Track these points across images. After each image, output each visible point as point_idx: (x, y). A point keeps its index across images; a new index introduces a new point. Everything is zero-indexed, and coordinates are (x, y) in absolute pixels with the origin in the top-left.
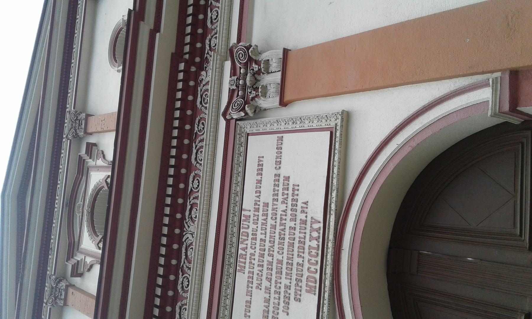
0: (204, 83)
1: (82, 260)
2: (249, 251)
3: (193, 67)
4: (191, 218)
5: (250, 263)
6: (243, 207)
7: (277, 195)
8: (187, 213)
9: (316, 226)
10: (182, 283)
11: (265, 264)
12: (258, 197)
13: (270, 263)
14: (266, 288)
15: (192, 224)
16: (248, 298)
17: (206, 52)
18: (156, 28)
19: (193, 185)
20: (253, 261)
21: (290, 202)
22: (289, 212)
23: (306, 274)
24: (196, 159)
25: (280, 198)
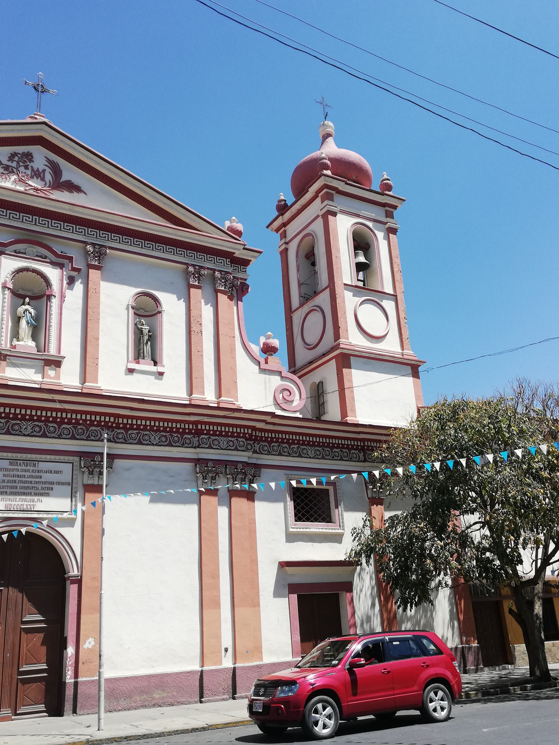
0: (102, 431)
2: (19, 468)
4: (34, 426)
5: (14, 469)
6: (39, 462)
8: (36, 423)
9: (32, 506)
11: (14, 479)
13: (15, 482)
14: (4, 480)
17: (117, 431)
19: (51, 427)
20: (15, 471)
23: (13, 503)
24: (64, 428)
25: (44, 486)
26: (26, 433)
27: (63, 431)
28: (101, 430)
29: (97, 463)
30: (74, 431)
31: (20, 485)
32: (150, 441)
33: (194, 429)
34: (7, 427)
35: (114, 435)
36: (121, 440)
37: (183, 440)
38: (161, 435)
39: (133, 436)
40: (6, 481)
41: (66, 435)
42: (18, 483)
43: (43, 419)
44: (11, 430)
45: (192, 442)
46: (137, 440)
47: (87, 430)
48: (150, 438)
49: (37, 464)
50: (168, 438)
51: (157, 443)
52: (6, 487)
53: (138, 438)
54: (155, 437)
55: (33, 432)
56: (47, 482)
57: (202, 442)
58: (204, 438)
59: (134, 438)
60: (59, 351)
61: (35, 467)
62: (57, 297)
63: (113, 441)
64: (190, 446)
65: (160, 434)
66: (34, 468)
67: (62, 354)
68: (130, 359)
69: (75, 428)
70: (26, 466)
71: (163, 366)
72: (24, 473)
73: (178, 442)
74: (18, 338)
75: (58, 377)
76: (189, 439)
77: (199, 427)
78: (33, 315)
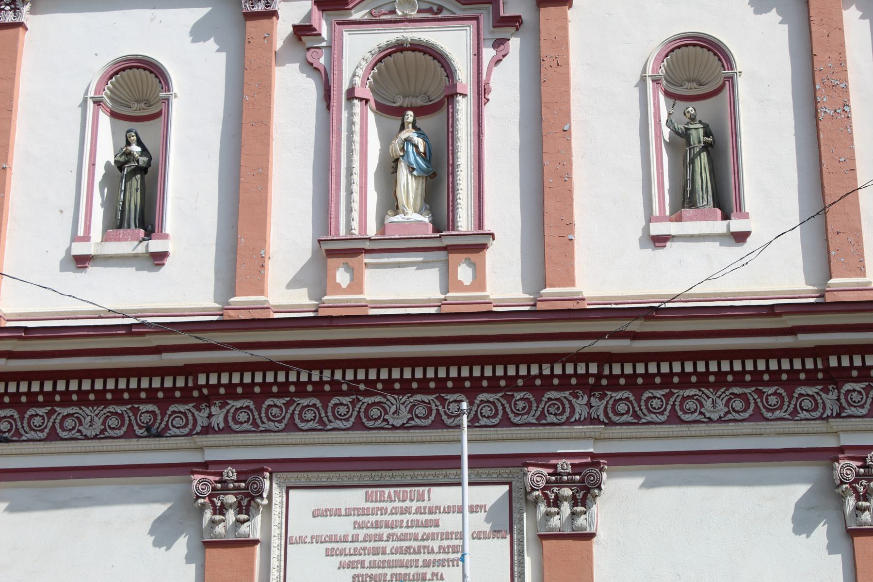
0: (574, 401)
1: (323, 40)
2: (389, 506)
3: (593, 381)
6: (434, 489)
7: (448, 539)
8: (419, 397)
10: (341, 404)
12: (445, 512)
15: (408, 408)
16: (343, 513)
17: (614, 394)
18: (635, 336)
19: (452, 402)
21: (442, 556)
22: (432, 557)
24: (482, 401)
25: (445, 543)
26: (398, 423)
27: (482, 409)
28: (571, 398)
29: (565, 478)
30: (507, 406)
31: (389, 545)
32: (701, 413)
33: (820, 370)
34: (355, 413)
35: (606, 407)
36: (625, 416)
37: (793, 402)
38: (731, 394)
39: (656, 403)
40: (361, 538)
41: (488, 417)
42: (388, 541)
43: (432, 385)
44: (364, 420)
45: (821, 406)
46: (667, 413)
47: (539, 402)
48: (702, 406)
49: (426, 493)
50: (752, 401)
51: (720, 417)
52: (362, 552)
53: (668, 410)
54: (713, 402)
55: (411, 419)
56: (452, 533)
57: (847, 401)
58: (854, 390)
59: (659, 408)
60: (480, 223)
61: (423, 500)
62: (469, 94)
63: (606, 421)
64: (817, 414)
65: (727, 393)
66: (420, 504)
67: (488, 227)
68: (656, 212)
69: (509, 398)
70: (404, 501)
71: (746, 216)
72: (398, 517)
73: (780, 408)
74: (397, 207)
75: (479, 282)
76: (812, 396)
77: (833, 362)
78: (422, 149)
